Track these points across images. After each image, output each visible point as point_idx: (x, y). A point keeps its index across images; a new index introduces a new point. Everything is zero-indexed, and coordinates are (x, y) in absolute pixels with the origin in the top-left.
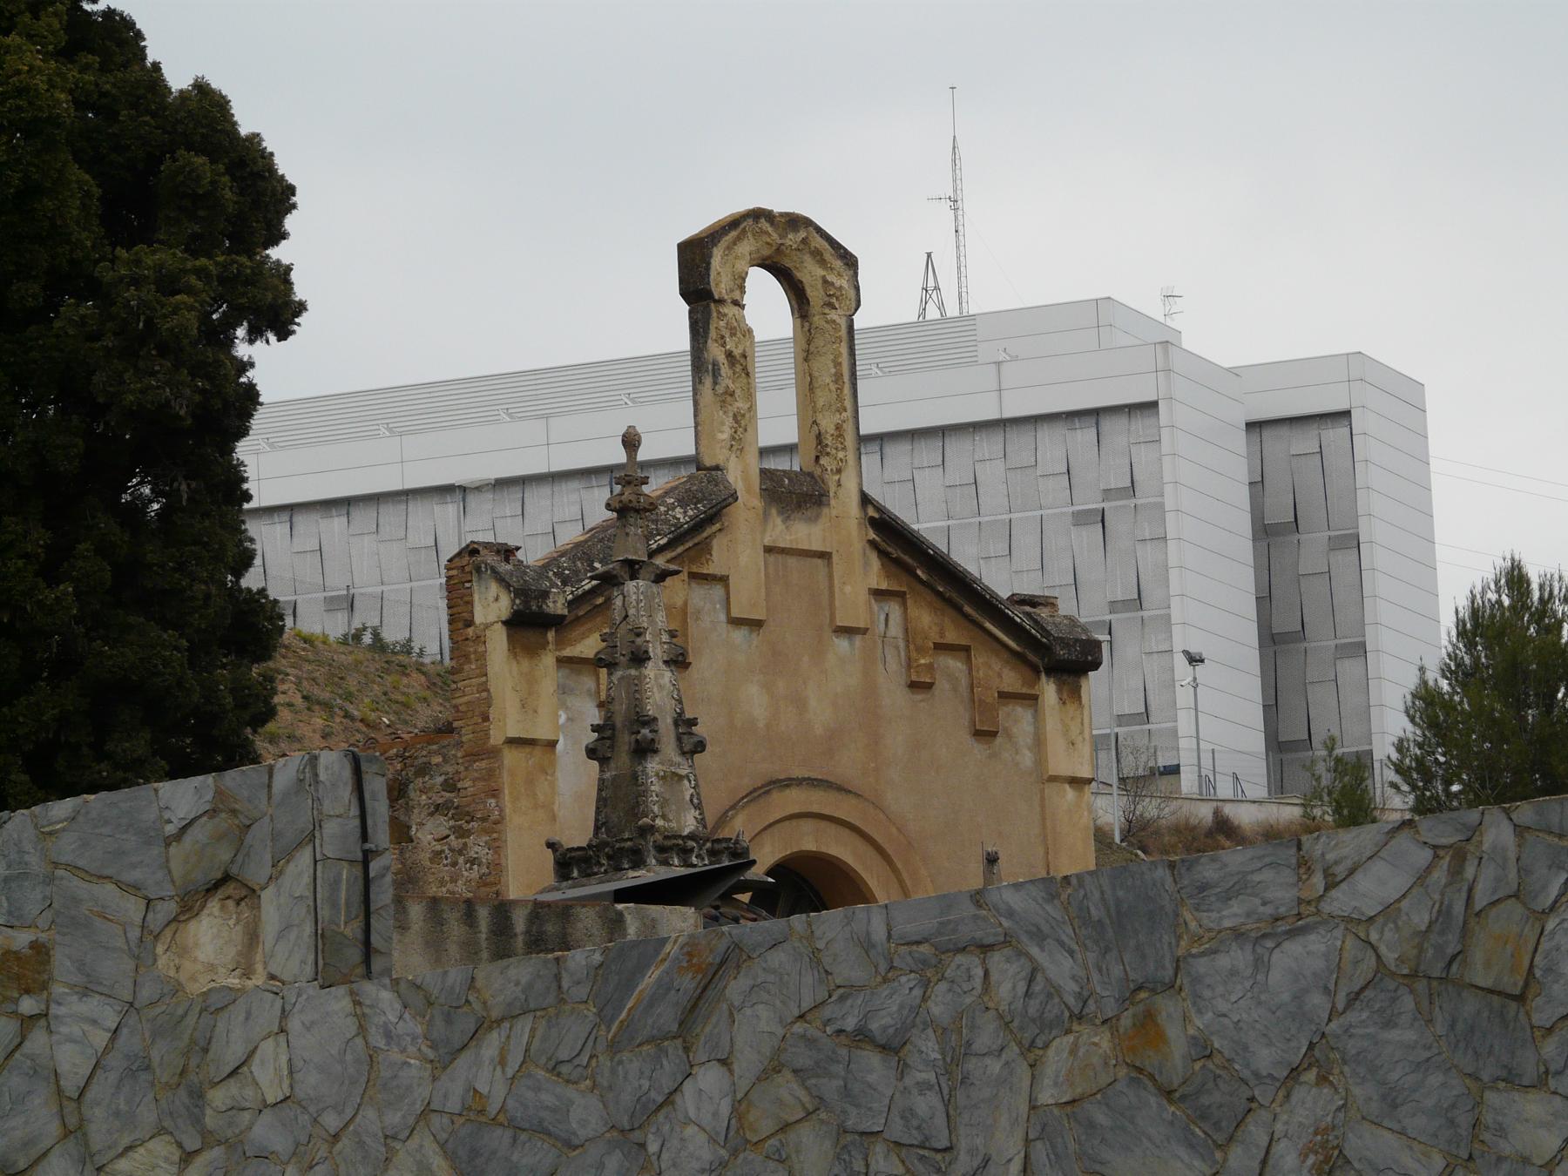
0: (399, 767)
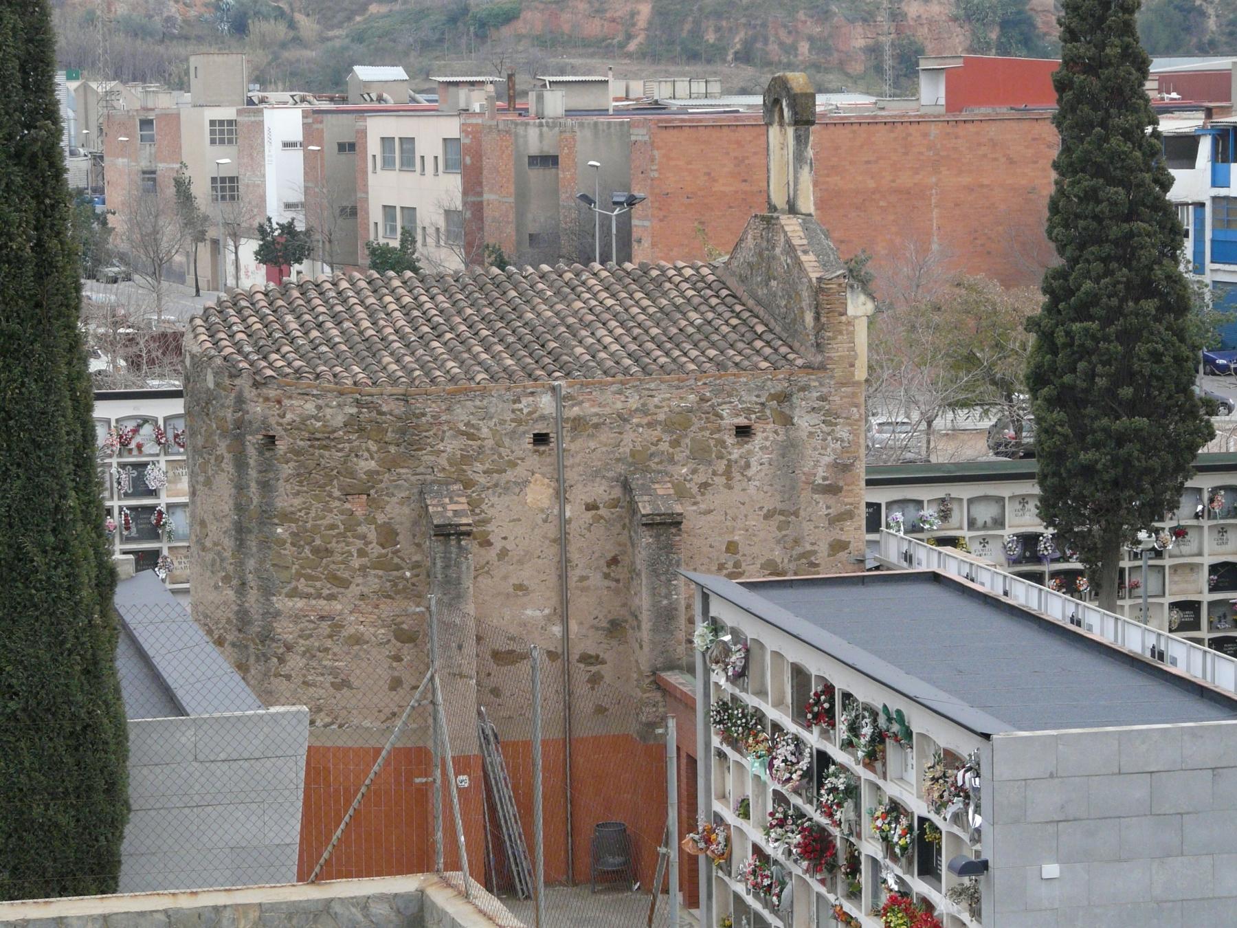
0: (786, 385)
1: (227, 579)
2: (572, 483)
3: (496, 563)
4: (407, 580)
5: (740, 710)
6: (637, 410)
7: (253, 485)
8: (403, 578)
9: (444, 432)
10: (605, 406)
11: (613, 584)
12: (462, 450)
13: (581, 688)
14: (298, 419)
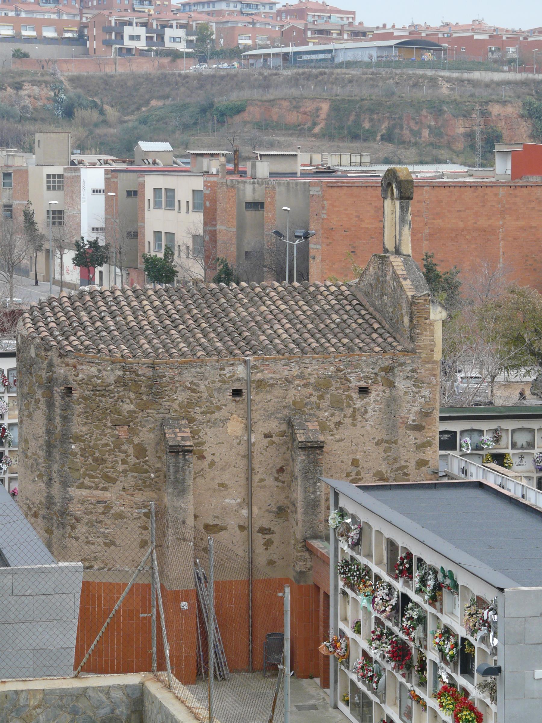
1: (40, 476)
2: (256, 420)
3: (208, 470)
4: (152, 479)
5: (356, 566)
6: (297, 376)
7: (58, 418)
8: (149, 477)
9: (177, 387)
10: (277, 373)
11: (280, 484)
12: (188, 399)
13: (259, 549)
14: (86, 378)
